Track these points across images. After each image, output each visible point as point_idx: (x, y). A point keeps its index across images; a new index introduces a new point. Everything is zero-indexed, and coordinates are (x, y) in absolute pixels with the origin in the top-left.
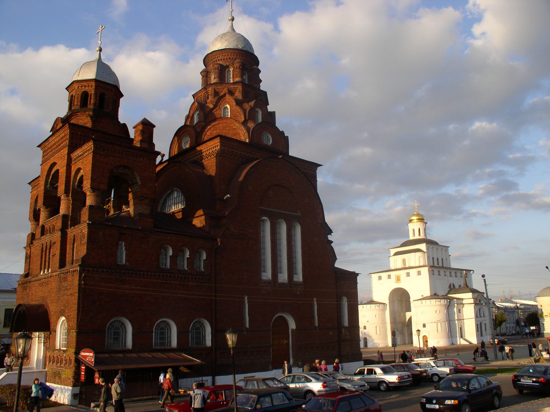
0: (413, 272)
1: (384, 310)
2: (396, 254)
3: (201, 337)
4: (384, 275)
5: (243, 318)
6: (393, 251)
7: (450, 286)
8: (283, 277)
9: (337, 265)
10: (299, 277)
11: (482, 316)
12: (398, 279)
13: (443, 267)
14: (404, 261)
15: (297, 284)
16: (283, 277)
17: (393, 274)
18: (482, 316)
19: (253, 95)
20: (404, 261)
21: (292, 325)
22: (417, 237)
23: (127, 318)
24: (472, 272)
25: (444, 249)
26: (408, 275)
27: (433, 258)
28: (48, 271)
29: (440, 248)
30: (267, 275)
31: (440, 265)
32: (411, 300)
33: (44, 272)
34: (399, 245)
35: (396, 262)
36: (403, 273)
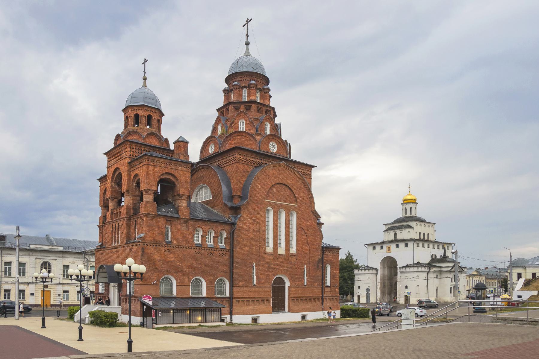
0: (402, 245)
3: (222, 290)
5: (252, 279)
7: (432, 256)
8: (282, 251)
9: (323, 241)
10: (293, 250)
12: (389, 249)
13: (428, 241)
14: (395, 234)
15: (292, 255)
16: (282, 251)
20: (395, 234)
21: (288, 284)
23: (173, 275)
25: (431, 225)
26: (397, 246)
27: (420, 233)
28: (118, 244)
30: (270, 249)
31: (426, 238)
33: (115, 244)
34: (392, 221)
36: (393, 246)
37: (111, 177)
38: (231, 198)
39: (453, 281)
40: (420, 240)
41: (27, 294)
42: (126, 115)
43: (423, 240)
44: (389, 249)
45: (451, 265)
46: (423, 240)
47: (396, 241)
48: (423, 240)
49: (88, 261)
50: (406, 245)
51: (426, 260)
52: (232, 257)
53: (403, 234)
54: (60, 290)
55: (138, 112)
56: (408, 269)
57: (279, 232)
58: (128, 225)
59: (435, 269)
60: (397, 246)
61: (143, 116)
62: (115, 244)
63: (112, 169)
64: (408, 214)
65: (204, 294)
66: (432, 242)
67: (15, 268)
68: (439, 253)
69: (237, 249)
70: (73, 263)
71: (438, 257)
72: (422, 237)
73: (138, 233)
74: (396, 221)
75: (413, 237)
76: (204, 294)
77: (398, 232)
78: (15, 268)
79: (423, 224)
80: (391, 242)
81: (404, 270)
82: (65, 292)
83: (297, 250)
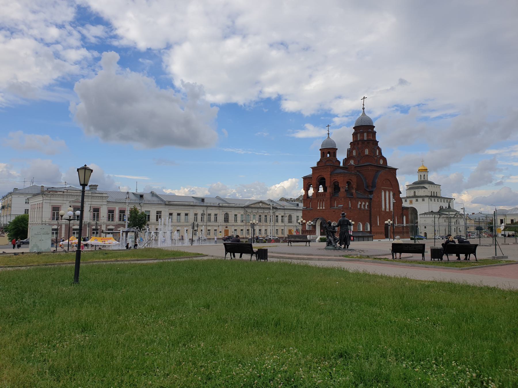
0: (420, 200)
8: (388, 210)
12: (411, 202)
14: (415, 192)
16: (388, 210)
20: (415, 192)
26: (417, 200)
29: (435, 186)
32: (418, 214)
36: (414, 200)
38: (368, 187)
40: (431, 196)
41: (218, 231)
43: (434, 197)
45: (454, 213)
46: (434, 197)
47: (415, 196)
48: (434, 197)
49: (246, 211)
50: (423, 200)
51: (436, 209)
52: (370, 214)
53: (420, 192)
54: (233, 228)
56: (426, 215)
57: (387, 202)
58: (331, 201)
59: (443, 216)
60: (417, 200)
64: (422, 179)
65: (361, 230)
66: (439, 197)
67: (213, 218)
68: (445, 205)
69: (372, 210)
70: (239, 213)
71: (444, 208)
72: (433, 195)
74: (415, 183)
75: (427, 195)
76: (361, 230)
77: (416, 190)
78: (213, 218)
79: (433, 186)
80: (412, 197)
82: (235, 230)
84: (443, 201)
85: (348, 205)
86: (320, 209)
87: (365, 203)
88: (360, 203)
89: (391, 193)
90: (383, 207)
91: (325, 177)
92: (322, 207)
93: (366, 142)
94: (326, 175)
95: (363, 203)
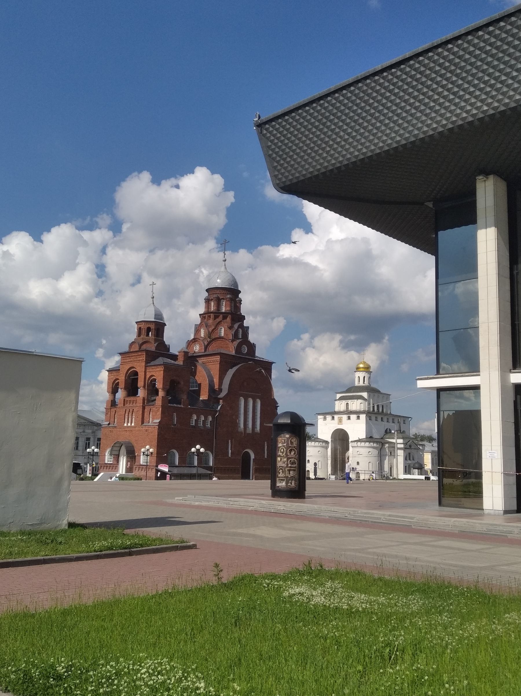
0: (353, 417)
1: (327, 448)
2: (341, 399)
4: (329, 418)
6: (338, 396)
11: (412, 459)
12: (340, 421)
15: (257, 433)
17: (336, 417)
18: (412, 459)
19: (237, 317)
21: (252, 456)
22: (361, 383)
24: (410, 419)
26: (349, 418)
29: (381, 396)
32: (350, 440)
33: (127, 425)
35: (340, 406)
36: (345, 417)
37: (125, 373)
39: (408, 459)
42: (140, 326)
44: (340, 421)
55: (150, 326)
56: (359, 443)
60: (349, 418)
61: (155, 328)
62: (127, 425)
63: (127, 367)
66: (386, 414)
73: (153, 419)
77: (350, 402)
79: (376, 395)
81: (355, 444)
83: (260, 429)
84: (391, 420)
85: (172, 419)
86: (128, 427)
87: (206, 418)
88: (195, 417)
89: (259, 402)
90: (242, 426)
91: (138, 369)
92: (131, 423)
93: (221, 316)
94: (140, 368)
95: (203, 418)
